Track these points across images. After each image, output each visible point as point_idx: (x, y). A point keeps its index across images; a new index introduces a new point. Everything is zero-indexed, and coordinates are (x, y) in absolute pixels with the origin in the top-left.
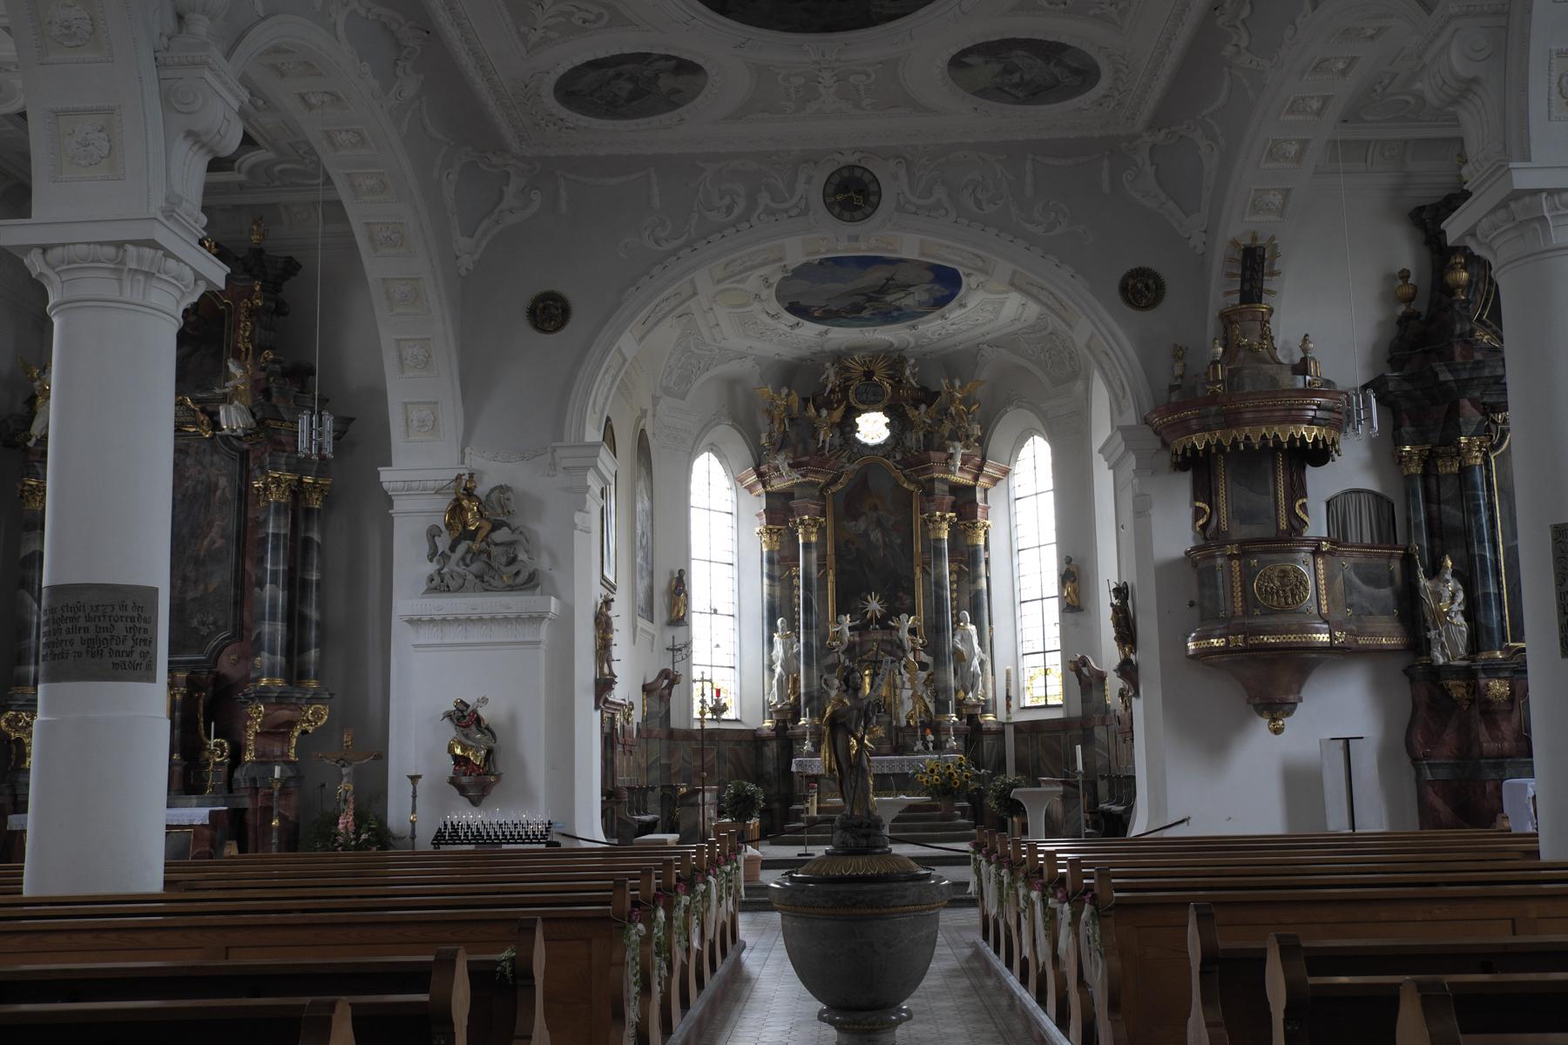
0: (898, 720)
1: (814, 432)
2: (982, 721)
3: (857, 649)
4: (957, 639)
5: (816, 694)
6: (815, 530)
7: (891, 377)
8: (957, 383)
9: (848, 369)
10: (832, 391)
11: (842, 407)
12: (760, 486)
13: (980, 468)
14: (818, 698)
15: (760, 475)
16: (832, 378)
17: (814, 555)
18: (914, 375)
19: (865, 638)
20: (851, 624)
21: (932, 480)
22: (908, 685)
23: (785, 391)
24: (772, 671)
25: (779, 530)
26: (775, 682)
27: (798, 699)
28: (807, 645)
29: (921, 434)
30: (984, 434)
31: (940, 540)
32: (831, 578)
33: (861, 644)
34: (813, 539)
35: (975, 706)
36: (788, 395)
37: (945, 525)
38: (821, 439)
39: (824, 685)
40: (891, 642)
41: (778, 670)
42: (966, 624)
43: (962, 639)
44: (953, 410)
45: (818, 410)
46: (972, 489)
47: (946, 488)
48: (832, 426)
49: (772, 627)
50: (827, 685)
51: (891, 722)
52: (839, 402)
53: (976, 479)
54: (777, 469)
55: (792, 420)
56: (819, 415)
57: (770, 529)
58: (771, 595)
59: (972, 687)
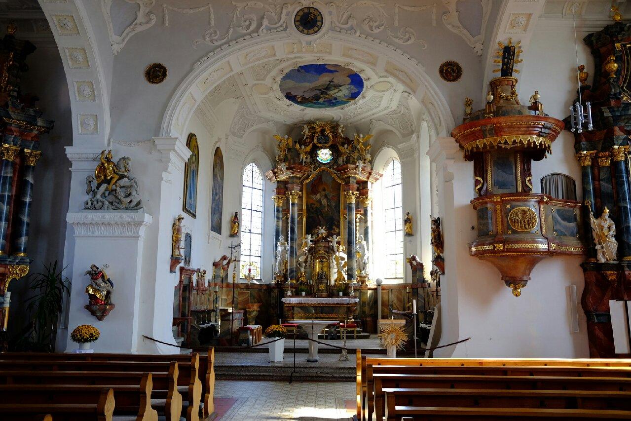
0: (330, 281)
1: (299, 154)
2: (367, 283)
3: (313, 250)
4: (358, 247)
5: (294, 270)
6: (297, 197)
7: (332, 132)
8: (361, 136)
9: (313, 128)
10: (307, 138)
11: (311, 145)
12: (274, 178)
13: (370, 173)
14: (296, 271)
15: (275, 173)
16: (307, 132)
17: (296, 208)
18: (342, 131)
19: (318, 245)
20: (311, 239)
21: (349, 177)
22: (336, 267)
23: (287, 137)
24: (276, 258)
25: (282, 197)
26: (277, 263)
27: (287, 271)
28: (292, 247)
29: (345, 157)
30: (372, 159)
31: (351, 203)
32: (304, 219)
33: (315, 248)
34: (296, 201)
35: (365, 277)
36: (288, 138)
37: (354, 197)
38: (301, 157)
39: (298, 266)
40: (328, 247)
41: (279, 258)
42: (362, 240)
43: (360, 248)
44: (359, 147)
45: (300, 146)
46: (366, 182)
47: (355, 181)
48: (306, 153)
49: (277, 239)
50: (300, 266)
51: (327, 283)
52: (310, 143)
53: (368, 178)
54: (281, 170)
55: (289, 149)
56: (301, 148)
57: (278, 197)
58: (278, 226)
59: (364, 268)
